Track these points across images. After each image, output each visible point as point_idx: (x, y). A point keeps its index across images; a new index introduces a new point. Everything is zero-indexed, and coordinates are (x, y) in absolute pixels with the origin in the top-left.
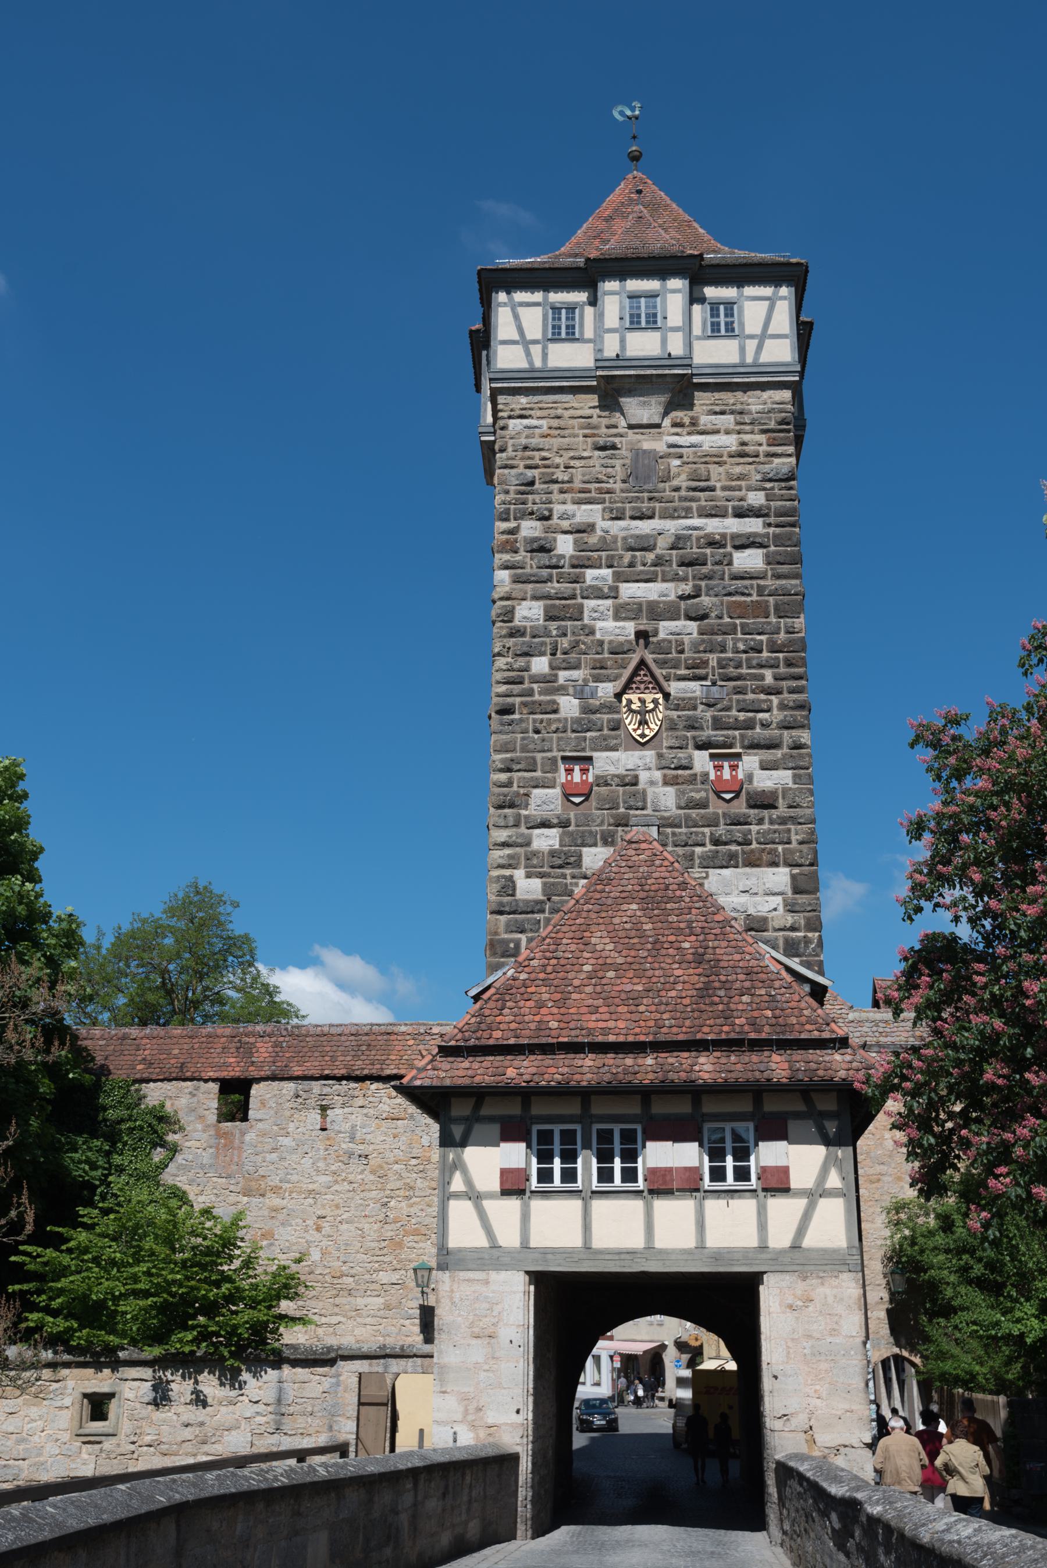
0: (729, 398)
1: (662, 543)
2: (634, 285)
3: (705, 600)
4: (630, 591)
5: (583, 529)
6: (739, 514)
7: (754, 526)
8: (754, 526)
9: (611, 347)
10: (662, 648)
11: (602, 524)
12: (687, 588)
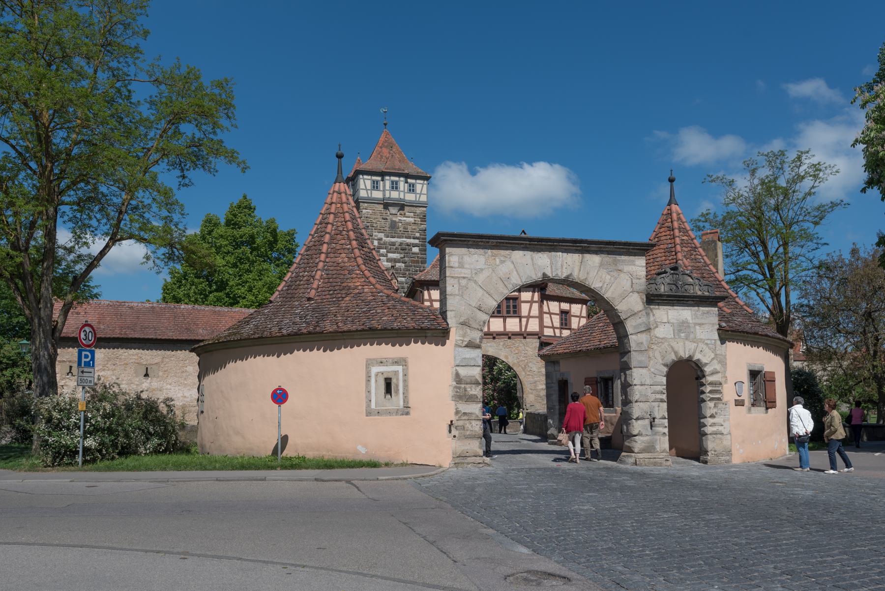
0: (413, 209)
1: (397, 244)
2: (393, 178)
3: (406, 259)
4: (390, 255)
5: (380, 239)
6: (414, 238)
7: (417, 241)
8: (417, 241)
9: (387, 195)
10: (397, 269)
11: (384, 239)
12: (402, 256)
